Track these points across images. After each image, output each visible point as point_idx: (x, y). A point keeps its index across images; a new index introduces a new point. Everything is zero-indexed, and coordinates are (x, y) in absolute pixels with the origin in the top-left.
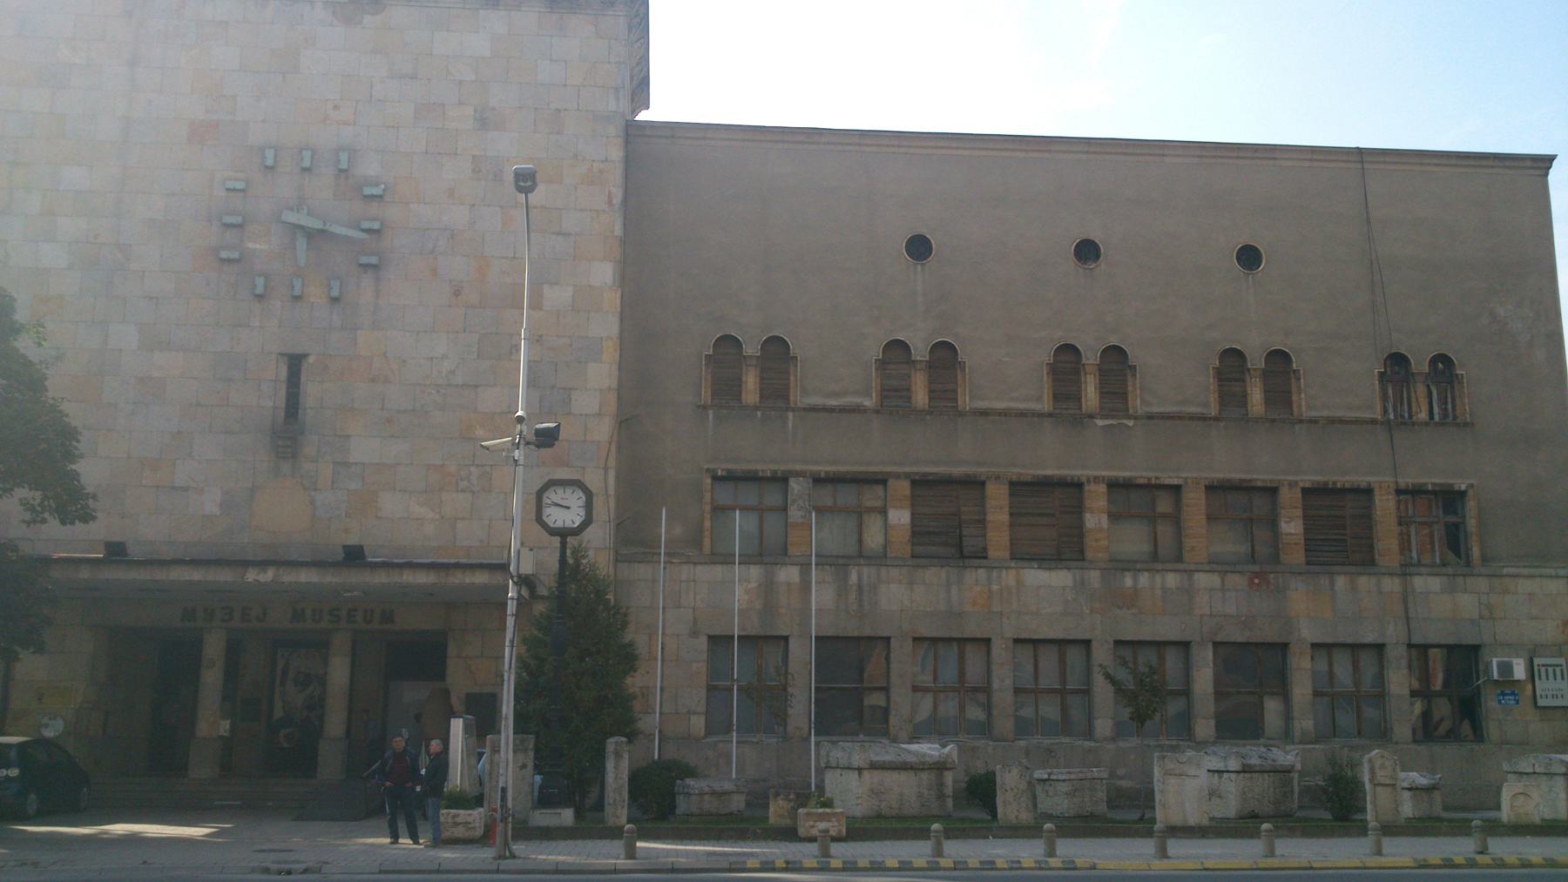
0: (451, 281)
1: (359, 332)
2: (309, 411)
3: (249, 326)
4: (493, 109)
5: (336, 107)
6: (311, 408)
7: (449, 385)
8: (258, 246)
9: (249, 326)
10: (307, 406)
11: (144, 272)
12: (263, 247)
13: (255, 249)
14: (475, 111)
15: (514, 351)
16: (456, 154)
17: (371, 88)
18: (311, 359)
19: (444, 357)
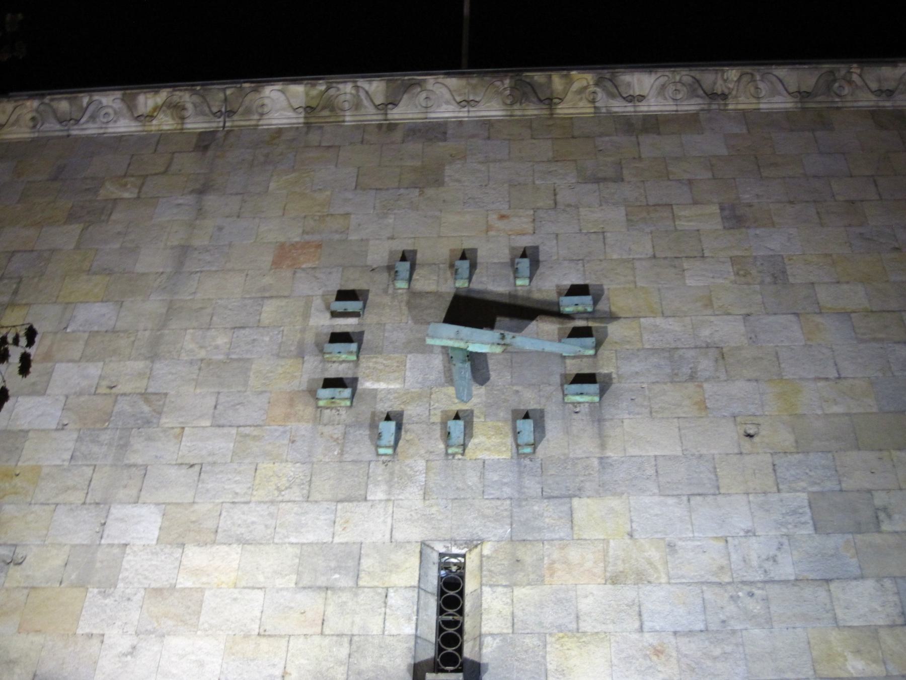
0: (734, 417)
1: (576, 502)
2: (488, 640)
3: (365, 499)
4: (750, 206)
5: (502, 217)
6: (491, 635)
7: (773, 581)
8: (382, 386)
9: (365, 499)
10: (484, 630)
11: (183, 428)
12: (392, 386)
13: (376, 390)
14: (722, 209)
15: (882, 516)
16: (703, 257)
17: (555, 195)
18: (487, 549)
19: (750, 533)
